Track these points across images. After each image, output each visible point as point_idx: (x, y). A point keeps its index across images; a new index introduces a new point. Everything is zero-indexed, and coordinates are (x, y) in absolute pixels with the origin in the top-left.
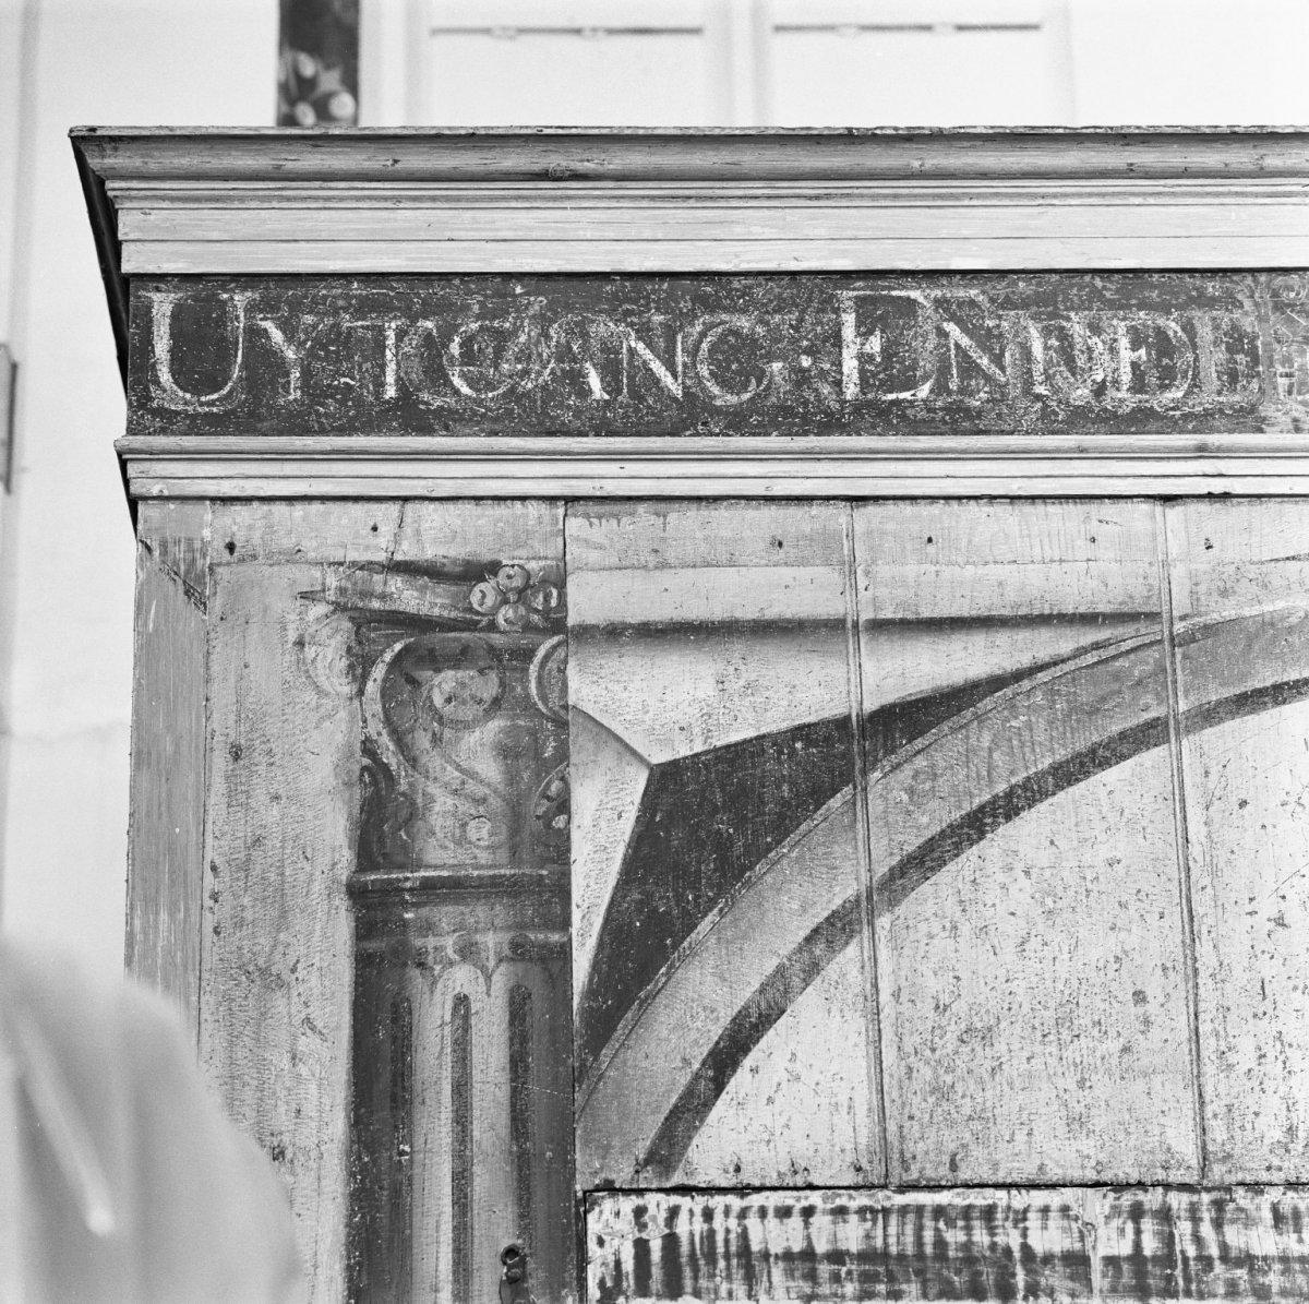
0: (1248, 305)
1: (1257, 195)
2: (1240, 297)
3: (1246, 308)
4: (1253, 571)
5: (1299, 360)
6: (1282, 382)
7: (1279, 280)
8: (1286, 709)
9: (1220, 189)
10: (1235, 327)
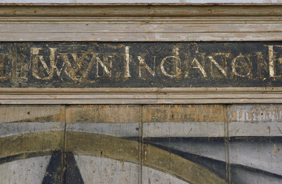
0: (10, 51)
1: (15, 21)
2: (8, 49)
3: (10, 52)
4: (5, 125)
5: (23, 67)
6: (17, 73)
7: (20, 45)
8: (10, 163)
9: (5, 20)
10: (6, 57)
